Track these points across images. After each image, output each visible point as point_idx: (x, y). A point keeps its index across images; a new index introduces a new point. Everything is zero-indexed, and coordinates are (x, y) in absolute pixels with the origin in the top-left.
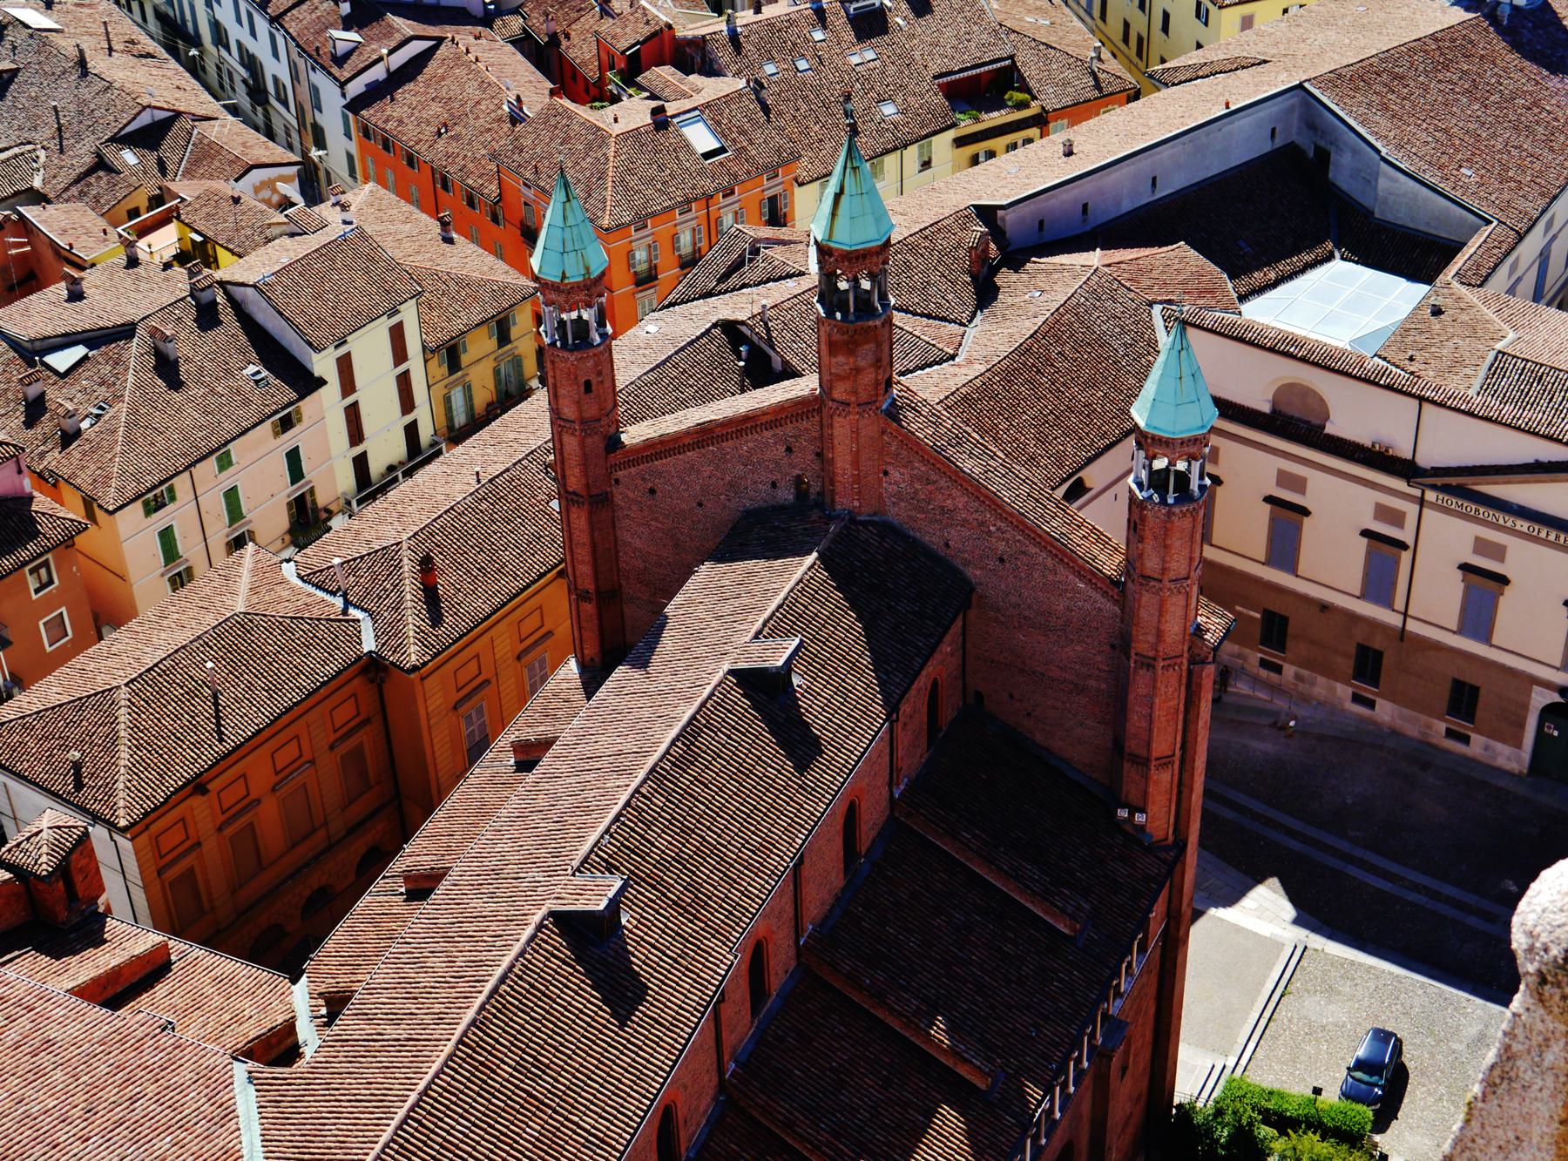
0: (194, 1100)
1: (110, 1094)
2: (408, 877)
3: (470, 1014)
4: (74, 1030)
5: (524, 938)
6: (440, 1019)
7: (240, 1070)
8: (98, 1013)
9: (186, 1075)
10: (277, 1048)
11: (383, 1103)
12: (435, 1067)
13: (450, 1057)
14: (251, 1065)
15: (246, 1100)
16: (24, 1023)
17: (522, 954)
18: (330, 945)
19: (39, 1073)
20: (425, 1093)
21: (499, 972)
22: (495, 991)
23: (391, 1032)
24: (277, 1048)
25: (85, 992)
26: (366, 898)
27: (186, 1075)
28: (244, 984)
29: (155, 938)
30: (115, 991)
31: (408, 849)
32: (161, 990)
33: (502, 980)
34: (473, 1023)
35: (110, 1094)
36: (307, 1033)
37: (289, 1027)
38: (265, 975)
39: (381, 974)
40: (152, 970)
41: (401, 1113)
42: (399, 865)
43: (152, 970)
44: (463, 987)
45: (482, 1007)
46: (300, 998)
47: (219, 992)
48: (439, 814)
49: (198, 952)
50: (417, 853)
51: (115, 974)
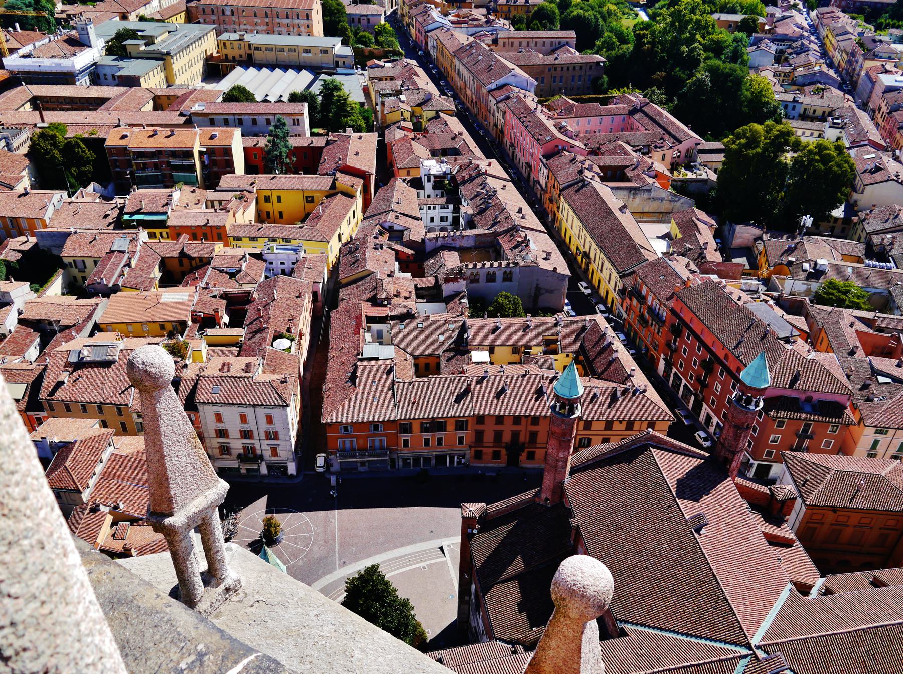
0: (772, 583)
1: (753, 563)
2: (875, 578)
3: (864, 627)
4: (756, 541)
5: (898, 621)
6: (854, 620)
7: (790, 586)
8: (765, 542)
9: (775, 575)
10: (804, 589)
11: (820, 628)
12: (843, 631)
13: (849, 632)
14: (793, 587)
15: (785, 594)
16: (746, 530)
17: (893, 625)
18: (839, 576)
19: (740, 544)
20: (835, 634)
21: (882, 624)
22: (877, 627)
23: (838, 611)
24: (804, 589)
25: (765, 534)
26: (858, 573)
27: (775, 575)
28: (807, 567)
29: (793, 536)
30: (774, 541)
31: (882, 571)
32: (785, 550)
33: (881, 626)
34: (863, 630)
35: (753, 563)
36: (814, 592)
37: (811, 587)
38: (815, 569)
39: (847, 595)
40: (786, 543)
41: (824, 634)
42: (875, 573)
43: (786, 543)
44: (868, 618)
45: (869, 628)
46: (820, 583)
47: (798, 563)
48: (898, 569)
49: (802, 549)
50: (883, 574)
51: (778, 536)
